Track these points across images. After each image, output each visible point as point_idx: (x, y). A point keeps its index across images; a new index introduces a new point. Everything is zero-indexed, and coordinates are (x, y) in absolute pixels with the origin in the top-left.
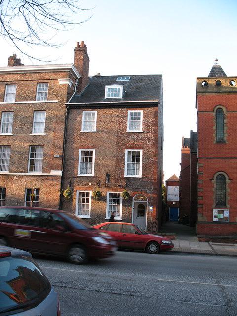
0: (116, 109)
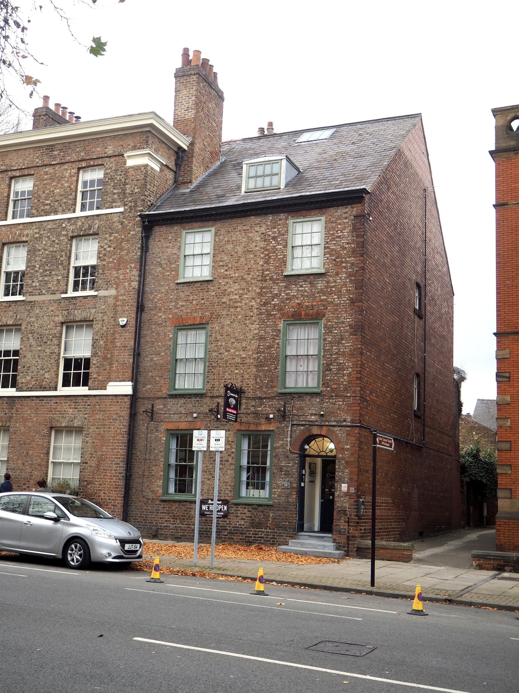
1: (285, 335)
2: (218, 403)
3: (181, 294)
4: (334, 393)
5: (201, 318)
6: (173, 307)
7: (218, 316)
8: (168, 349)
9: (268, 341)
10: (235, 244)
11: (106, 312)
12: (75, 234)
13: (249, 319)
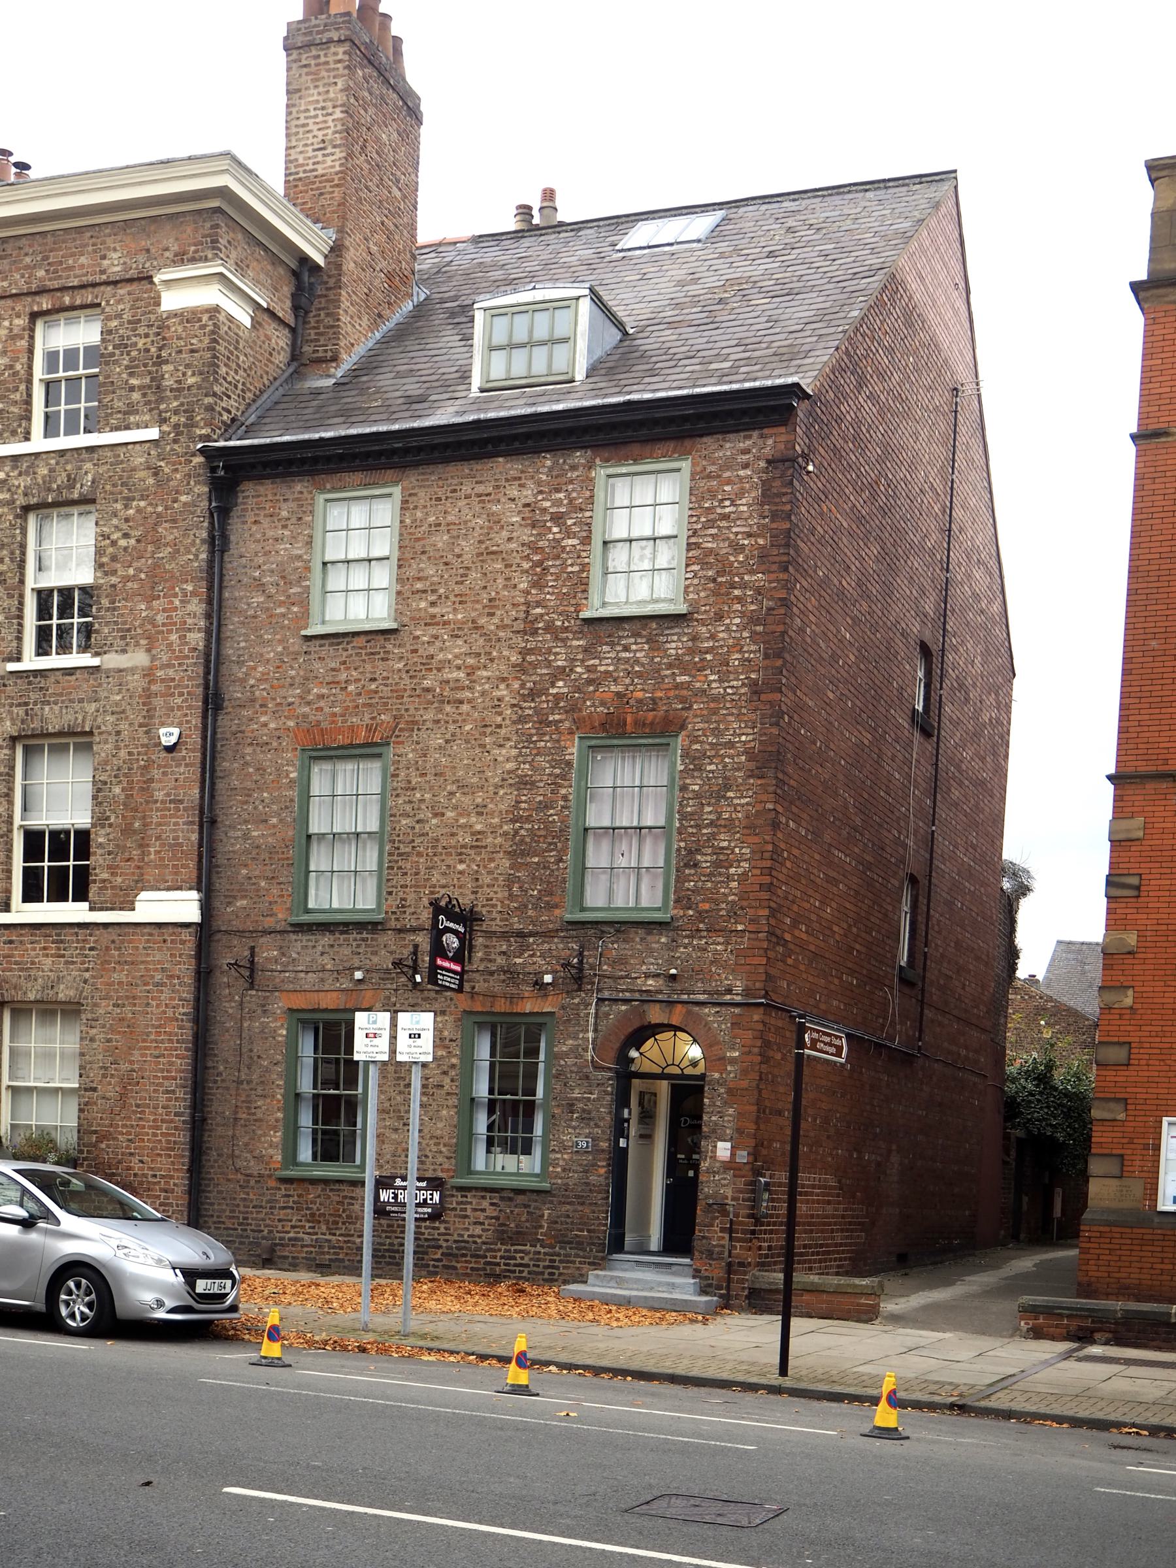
1: (583, 774)
2: (416, 947)
3: (317, 665)
5: (369, 728)
6: (297, 701)
7: (414, 725)
9: (541, 791)
10: (455, 533)
12: (33, 501)
13: (491, 734)
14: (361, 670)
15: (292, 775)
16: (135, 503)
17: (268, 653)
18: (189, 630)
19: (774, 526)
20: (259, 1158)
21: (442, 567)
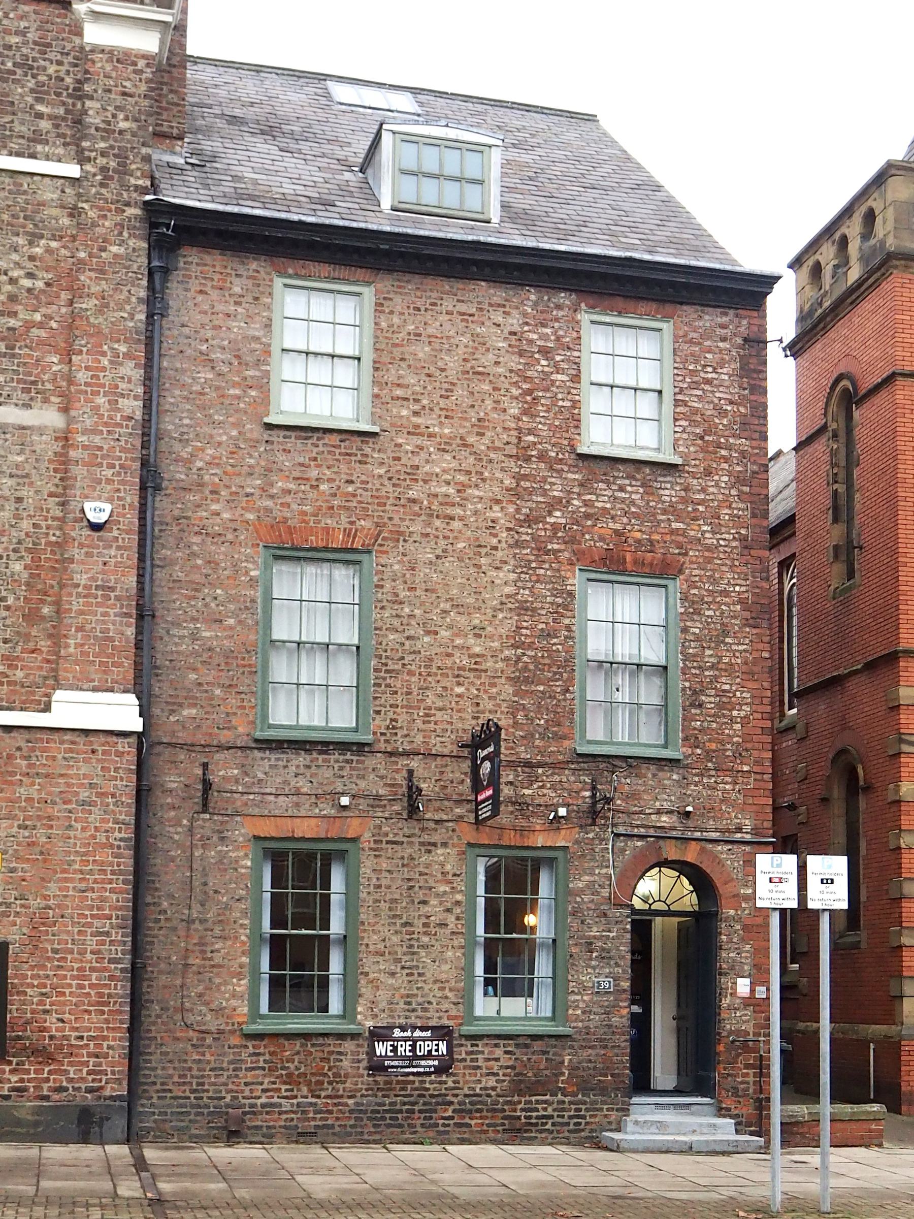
0: (498, 294)
2: (411, 772)
3: (281, 457)
4: (711, 761)
6: (258, 492)
7: (398, 536)
8: (247, 608)
9: (543, 619)
10: (437, 347)
11: (27, 476)
13: (486, 554)
14: (336, 469)
15: (252, 573)
16: (43, 242)
17: (220, 435)
18: (123, 396)
19: (753, 398)
20: (218, 1012)
21: (424, 378)
